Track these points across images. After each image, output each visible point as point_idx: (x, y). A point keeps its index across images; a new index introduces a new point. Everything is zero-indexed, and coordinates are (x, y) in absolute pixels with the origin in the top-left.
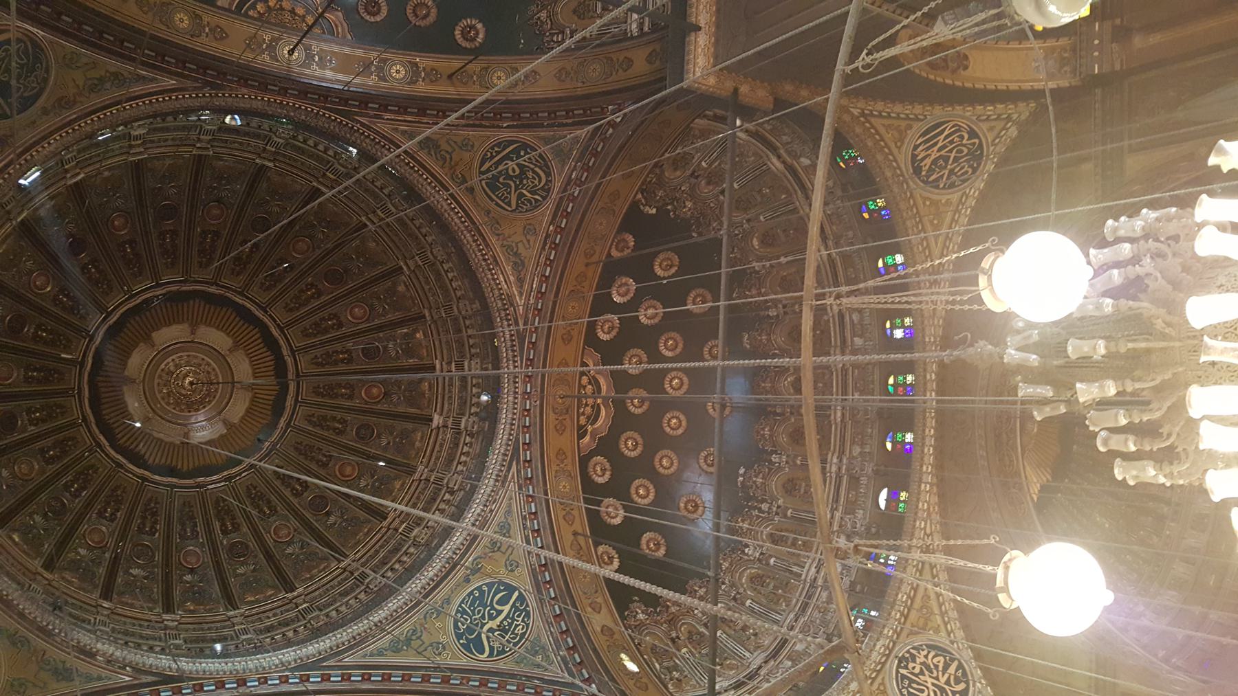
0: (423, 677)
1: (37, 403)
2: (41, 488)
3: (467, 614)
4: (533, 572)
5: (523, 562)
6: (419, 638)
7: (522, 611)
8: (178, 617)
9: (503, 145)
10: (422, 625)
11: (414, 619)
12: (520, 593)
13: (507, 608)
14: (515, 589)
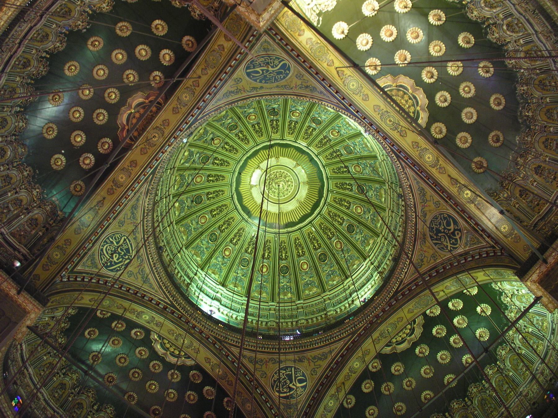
7: (253, 65)
10: (296, 87)
12: (247, 69)
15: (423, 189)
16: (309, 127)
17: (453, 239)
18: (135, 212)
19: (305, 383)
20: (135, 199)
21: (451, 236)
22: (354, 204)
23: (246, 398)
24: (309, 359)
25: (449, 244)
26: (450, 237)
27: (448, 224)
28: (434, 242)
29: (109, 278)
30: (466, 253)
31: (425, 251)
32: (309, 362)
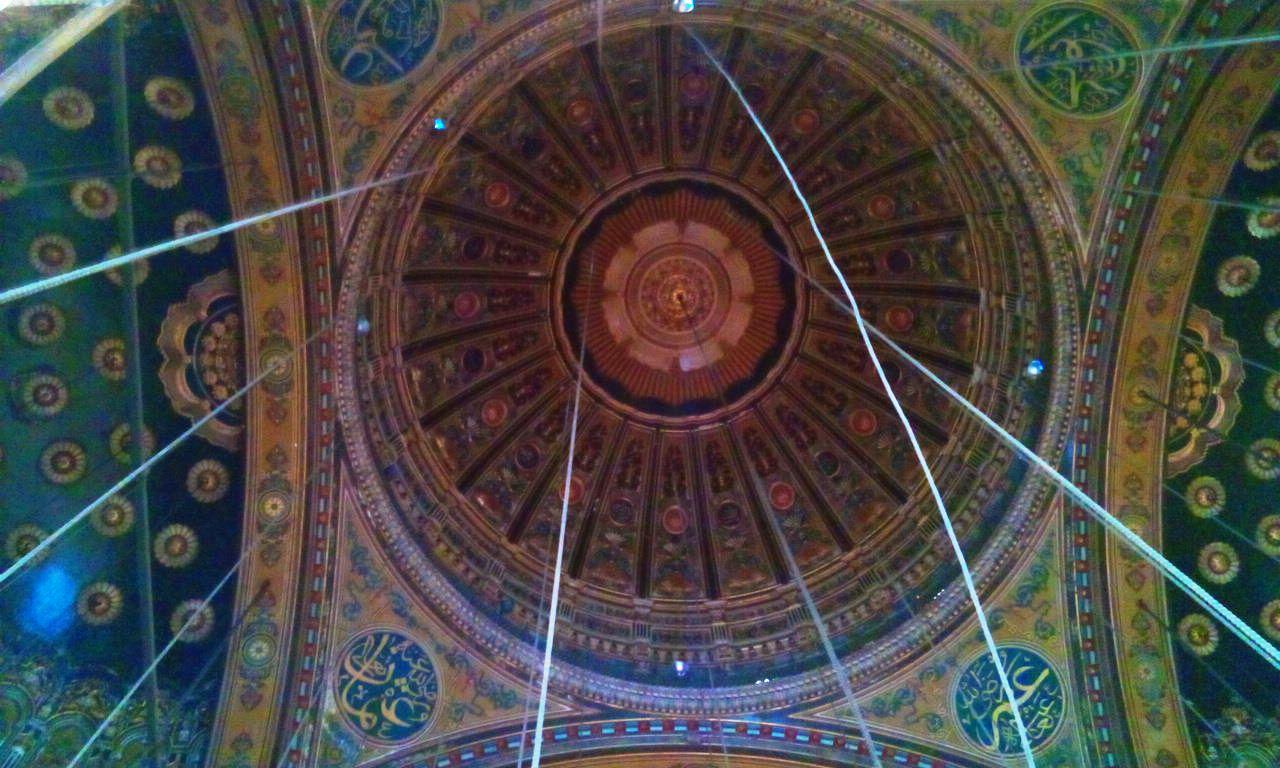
0: (909, 757)
1: (503, 333)
2: (512, 434)
3: (977, 686)
5: (1061, 627)
6: (911, 703)
7: (1051, 699)
12: (1051, 672)
13: (1030, 690)
14: (1045, 666)
15: (507, 706)
16: (730, 482)
17: (366, 698)
18: (1075, 180)
19: (345, 63)
20: (1097, 212)
21: (372, 697)
22: (512, 414)
24: (382, 120)
25: (358, 675)
26: (375, 692)
27: (402, 711)
30: (315, 712)
31: (378, 596)
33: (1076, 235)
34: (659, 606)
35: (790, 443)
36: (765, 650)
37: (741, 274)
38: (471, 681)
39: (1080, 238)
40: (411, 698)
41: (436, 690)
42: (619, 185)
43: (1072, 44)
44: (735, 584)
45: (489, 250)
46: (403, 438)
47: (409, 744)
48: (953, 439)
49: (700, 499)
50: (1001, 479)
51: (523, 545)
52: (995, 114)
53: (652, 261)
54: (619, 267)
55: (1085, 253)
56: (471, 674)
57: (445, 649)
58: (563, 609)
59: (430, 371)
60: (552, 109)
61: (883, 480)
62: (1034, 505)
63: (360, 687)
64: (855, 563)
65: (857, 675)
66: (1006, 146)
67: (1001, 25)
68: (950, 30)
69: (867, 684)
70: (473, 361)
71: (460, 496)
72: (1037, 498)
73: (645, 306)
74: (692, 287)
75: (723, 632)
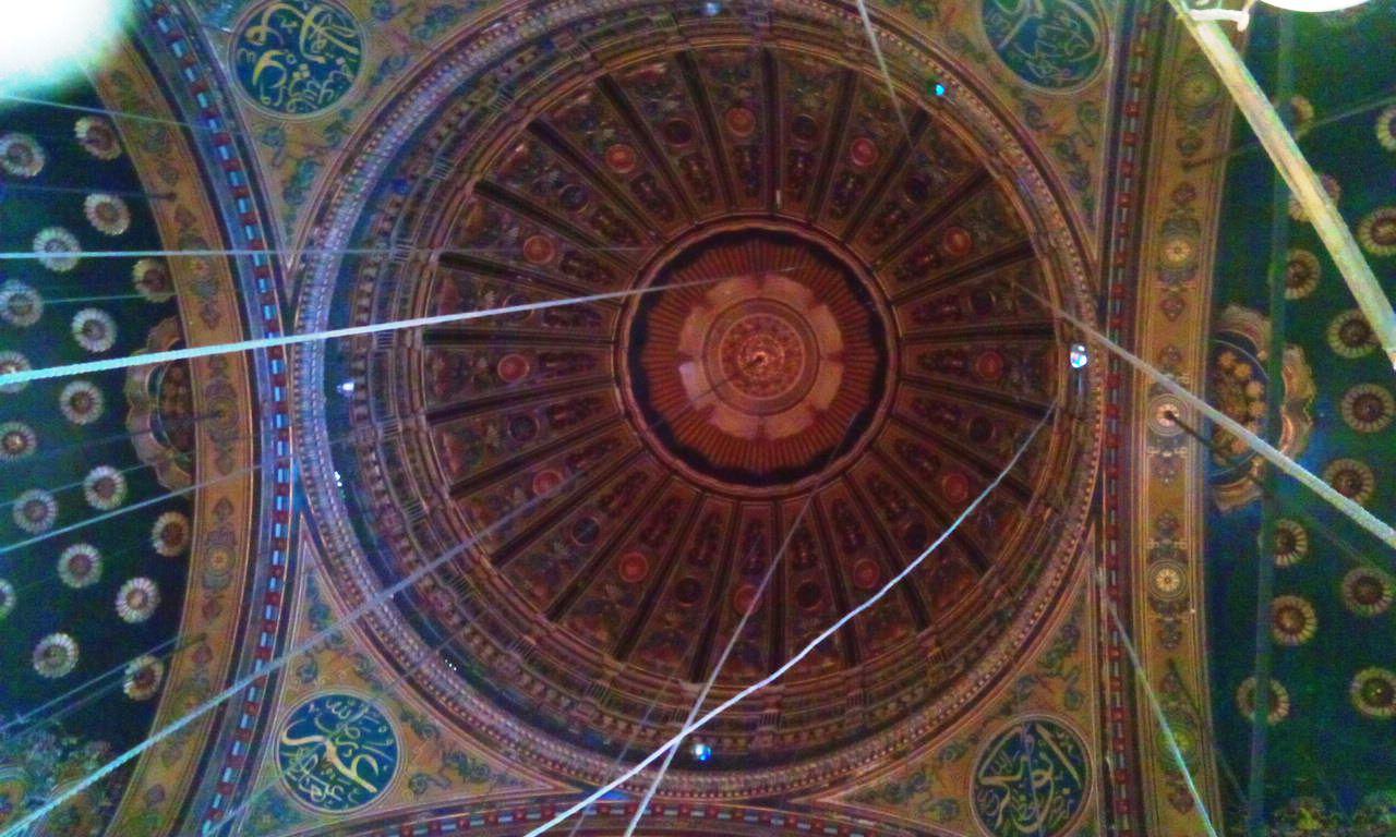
2: (598, 178)
4: (402, 817)
5: (423, 801)
7: (344, 797)
8: (418, 346)
9: (1077, 757)
11: (357, 641)
12: (373, 795)
14: (380, 788)
15: (286, 195)
18: (903, 786)
22: (621, 179)
23: (1179, 117)
24: (944, 26)
25: (308, 21)
27: (270, 75)
28: (353, 50)
29: (1105, 764)
31: (404, 39)
32: (948, 19)
33: (847, 788)
34: (415, 355)
35: (606, 490)
36: (374, 480)
37: (786, 426)
38: (311, 153)
39: (842, 793)
40: (287, 84)
41: (298, 112)
42: (880, 287)
43: (1048, 776)
44: (446, 439)
45: (803, 145)
46: (587, 55)
47: (233, 85)
48: (621, 666)
49: (537, 395)
50: (582, 722)
51: (473, 200)
52: (970, 697)
53: (799, 327)
54: (787, 289)
55: (828, 800)
56: (320, 151)
57: (346, 120)
58: (385, 337)
59: (663, 84)
60: (960, 211)
61: (573, 591)
62: (555, 762)
63: (295, 24)
64: (478, 569)
65: (353, 586)
66: (935, 710)
67: (1066, 699)
68: (1059, 646)
69: (344, 595)
70: (678, 132)
71: (524, 125)
72: (562, 765)
73: (749, 322)
74: (772, 373)
75: (390, 430)
